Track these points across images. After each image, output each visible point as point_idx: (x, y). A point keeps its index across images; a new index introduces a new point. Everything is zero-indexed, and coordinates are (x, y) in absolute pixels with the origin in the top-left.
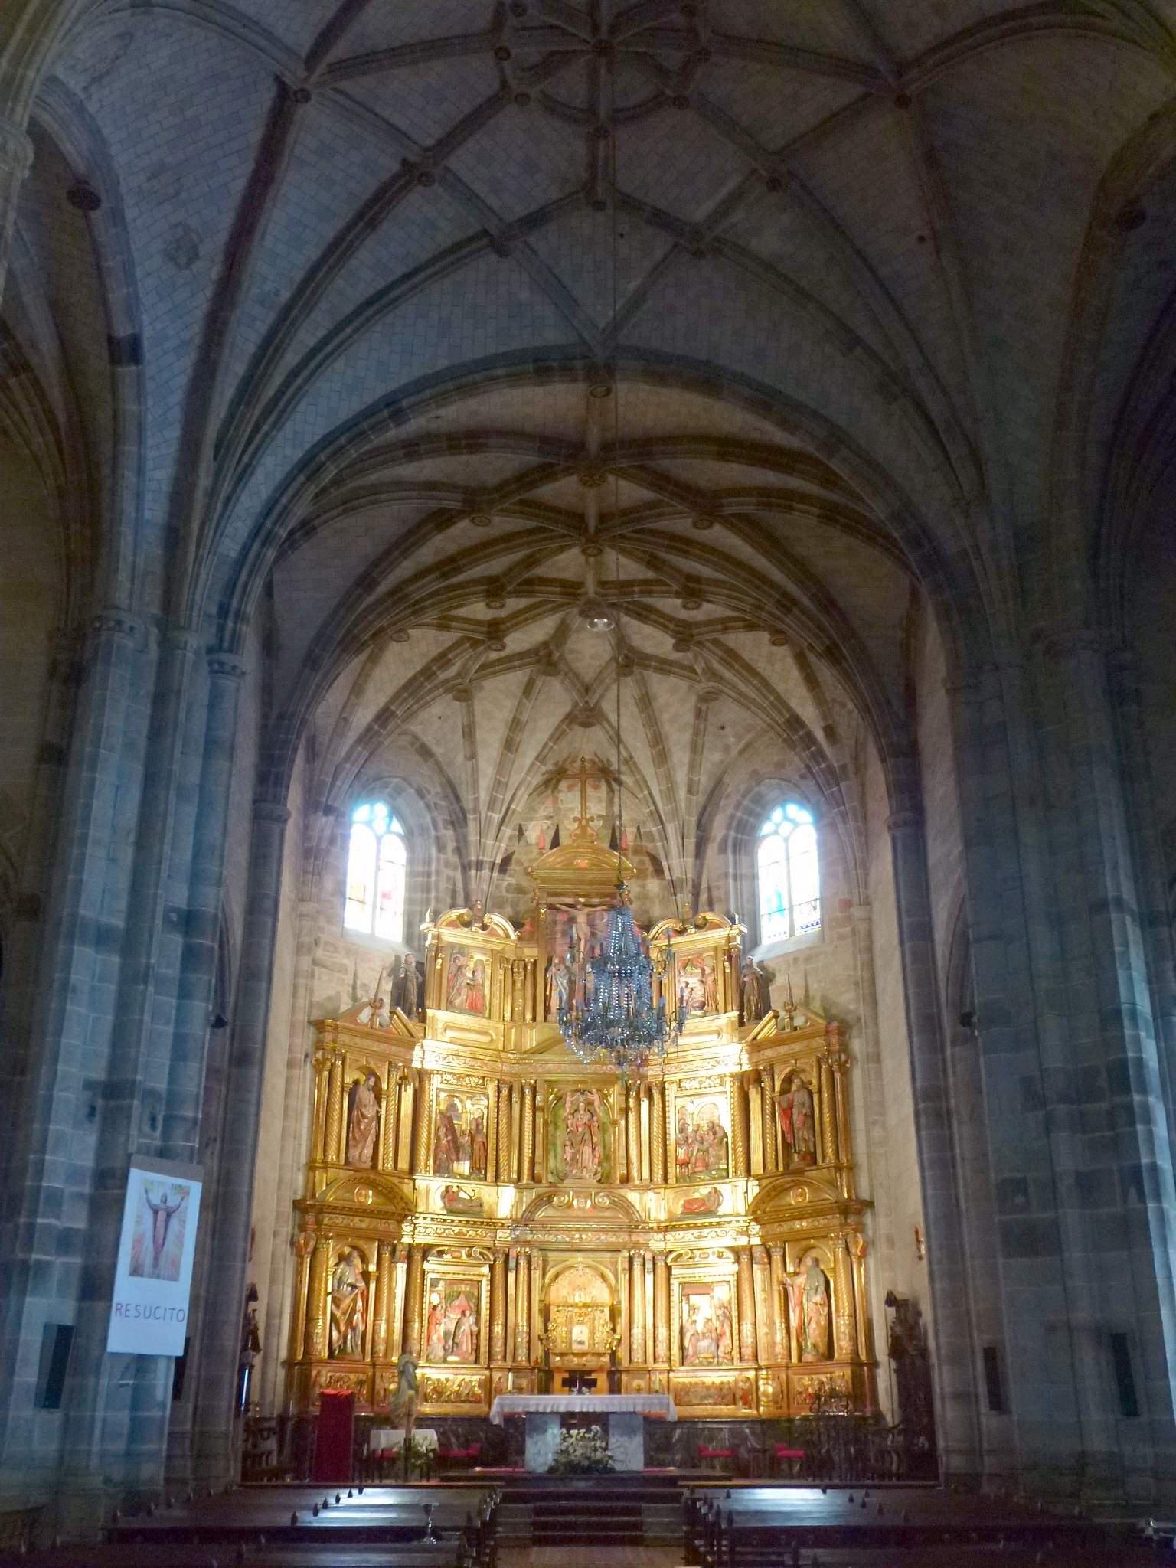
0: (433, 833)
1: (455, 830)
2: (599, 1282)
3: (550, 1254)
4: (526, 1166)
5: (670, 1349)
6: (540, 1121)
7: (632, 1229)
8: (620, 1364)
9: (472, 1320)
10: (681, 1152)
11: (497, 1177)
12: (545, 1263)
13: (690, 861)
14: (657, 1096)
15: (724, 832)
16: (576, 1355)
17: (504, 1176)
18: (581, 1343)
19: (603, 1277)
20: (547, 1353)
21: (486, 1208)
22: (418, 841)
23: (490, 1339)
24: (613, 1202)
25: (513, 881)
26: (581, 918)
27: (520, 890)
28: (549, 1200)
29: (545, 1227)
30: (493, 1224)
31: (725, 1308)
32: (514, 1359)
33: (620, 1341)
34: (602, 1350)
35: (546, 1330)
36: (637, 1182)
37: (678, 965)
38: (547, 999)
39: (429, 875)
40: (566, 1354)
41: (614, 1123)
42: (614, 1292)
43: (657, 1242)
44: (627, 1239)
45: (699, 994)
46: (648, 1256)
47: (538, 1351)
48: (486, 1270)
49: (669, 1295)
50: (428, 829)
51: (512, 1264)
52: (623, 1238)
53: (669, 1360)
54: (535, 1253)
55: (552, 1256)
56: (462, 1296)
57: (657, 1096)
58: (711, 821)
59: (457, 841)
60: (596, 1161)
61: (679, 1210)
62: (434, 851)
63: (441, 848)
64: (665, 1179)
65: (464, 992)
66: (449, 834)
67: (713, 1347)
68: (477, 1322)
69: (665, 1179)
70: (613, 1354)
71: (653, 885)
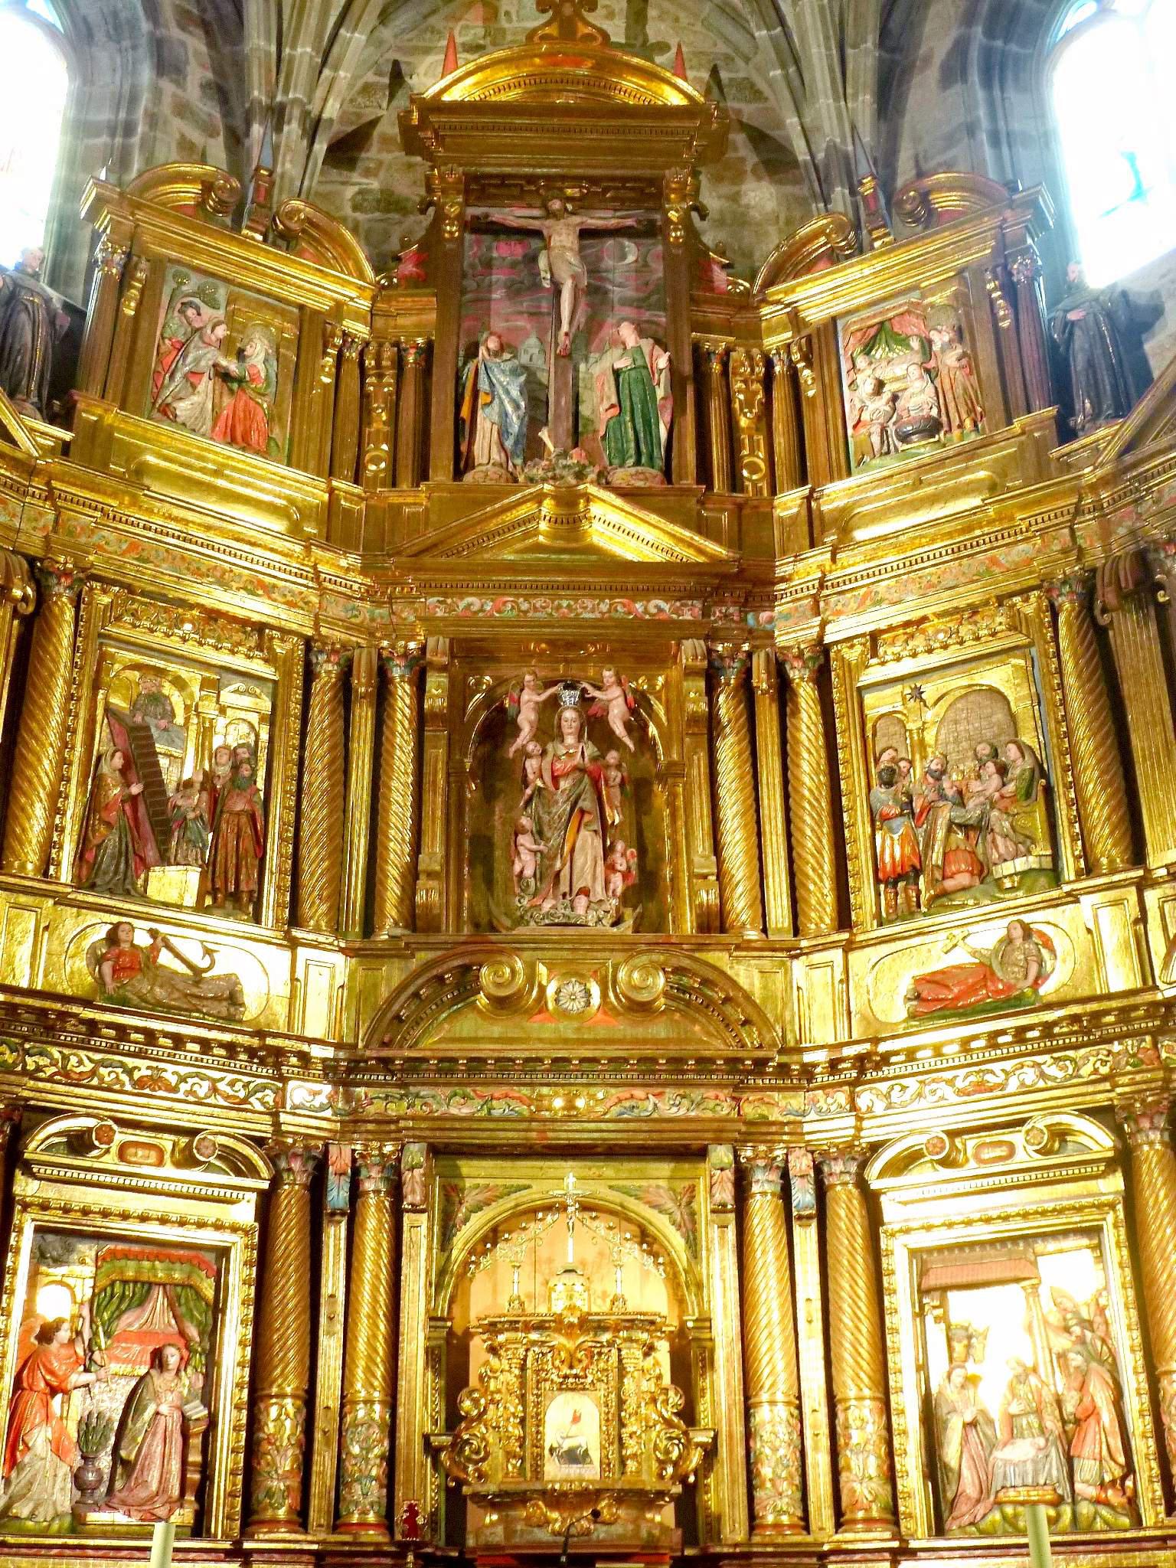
0: (145, 26)
1: (211, 44)
2: (633, 1254)
3: (468, 1168)
4: (392, 891)
5: (891, 1476)
6: (437, 754)
7: (746, 1072)
8: (714, 1525)
9: (191, 1379)
10: (893, 848)
11: (295, 919)
12: (452, 1194)
13: (864, 103)
14: (806, 694)
15: (954, 33)
16: (557, 1499)
17: (316, 909)
18: (574, 1457)
19: (645, 1237)
20: (455, 1499)
21: (252, 1009)
22: (104, 55)
23: (252, 1449)
24: (678, 993)
25: (374, 184)
26: (563, 237)
27: (389, 203)
28: (465, 984)
29: (448, 1070)
30: (269, 1054)
31: (1088, 1327)
32: (337, 1522)
33: (711, 1452)
34: (650, 1483)
35: (454, 1419)
36: (752, 934)
37: (848, 345)
38: (463, 430)
39: (129, 129)
40: (520, 1498)
41: (674, 772)
42: (684, 1284)
43: (826, 1118)
44: (725, 1109)
45: (919, 399)
46: (801, 1163)
47: (425, 1492)
48: (245, 1212)
49: (878, 1292)
50: (133, 24)
51: (337, 1194)
52: (713, 1104)
53: (893, 1515)
54: (416, 1153)
55: (475, 1173)
56: (159, 1299)
57: (806, 694)
58: (912, 25)
59: (218, 70)
60: (618, 883)
61: (894, 1010)
62: (146, 74)
63: (167, 64)
64: (844, 919)
65: (206, 385)
66: (194, 45)
67: (1055, 1468)
68: (208, 1394)
69: (844, 919)
70: (688, 1502)
71: (761, 196)
